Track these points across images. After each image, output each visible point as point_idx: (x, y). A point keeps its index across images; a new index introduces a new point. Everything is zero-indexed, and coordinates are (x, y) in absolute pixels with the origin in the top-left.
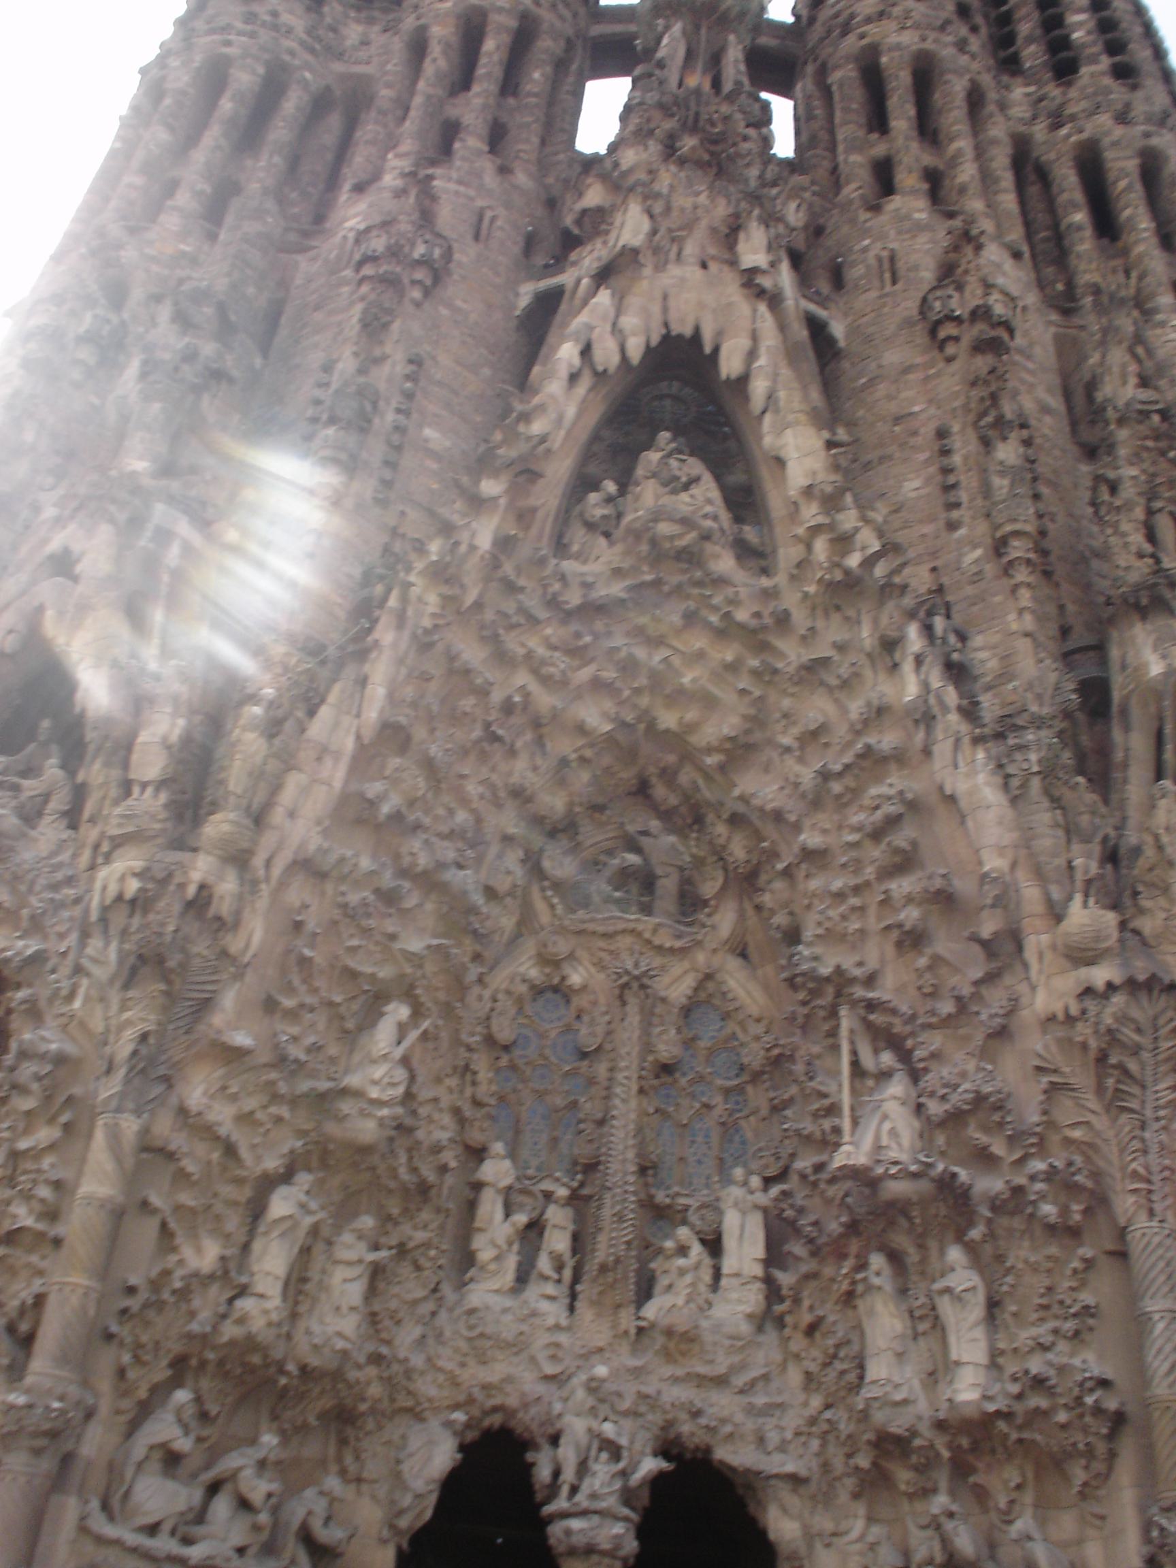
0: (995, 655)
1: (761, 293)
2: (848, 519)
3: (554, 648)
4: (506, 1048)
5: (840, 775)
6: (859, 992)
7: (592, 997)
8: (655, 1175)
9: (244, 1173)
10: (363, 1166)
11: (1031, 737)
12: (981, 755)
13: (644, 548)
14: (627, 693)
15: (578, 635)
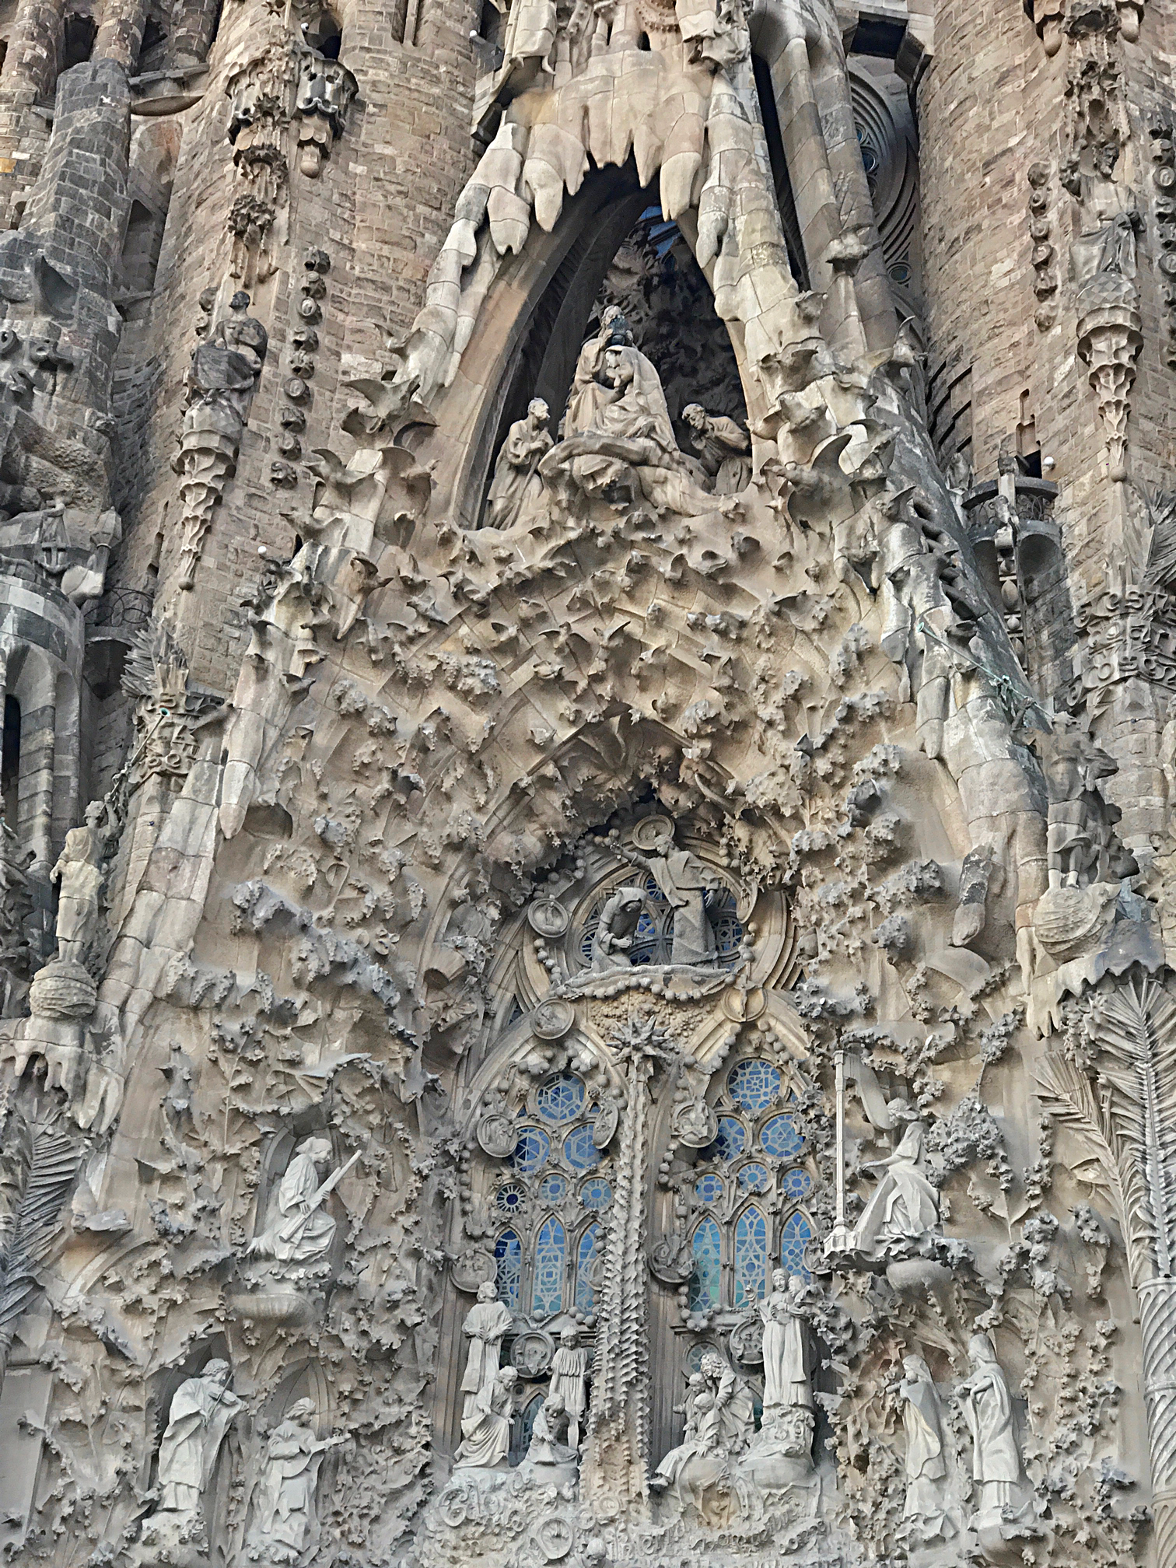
0: (1083, 515)
1: (715, 69)
2: (807, 400)
3: (476, 651)
4: (509, 1161)
5: (825, 747)
6: (858, 1028)
7: (601, 1079)
8: (694, 1292)
9: (137, 1373)
10: (292, 1340)
11: (1113, 631)
12: (975, 691)
13: (563, 496)
14: (583, 684)
15: (498, 628)
